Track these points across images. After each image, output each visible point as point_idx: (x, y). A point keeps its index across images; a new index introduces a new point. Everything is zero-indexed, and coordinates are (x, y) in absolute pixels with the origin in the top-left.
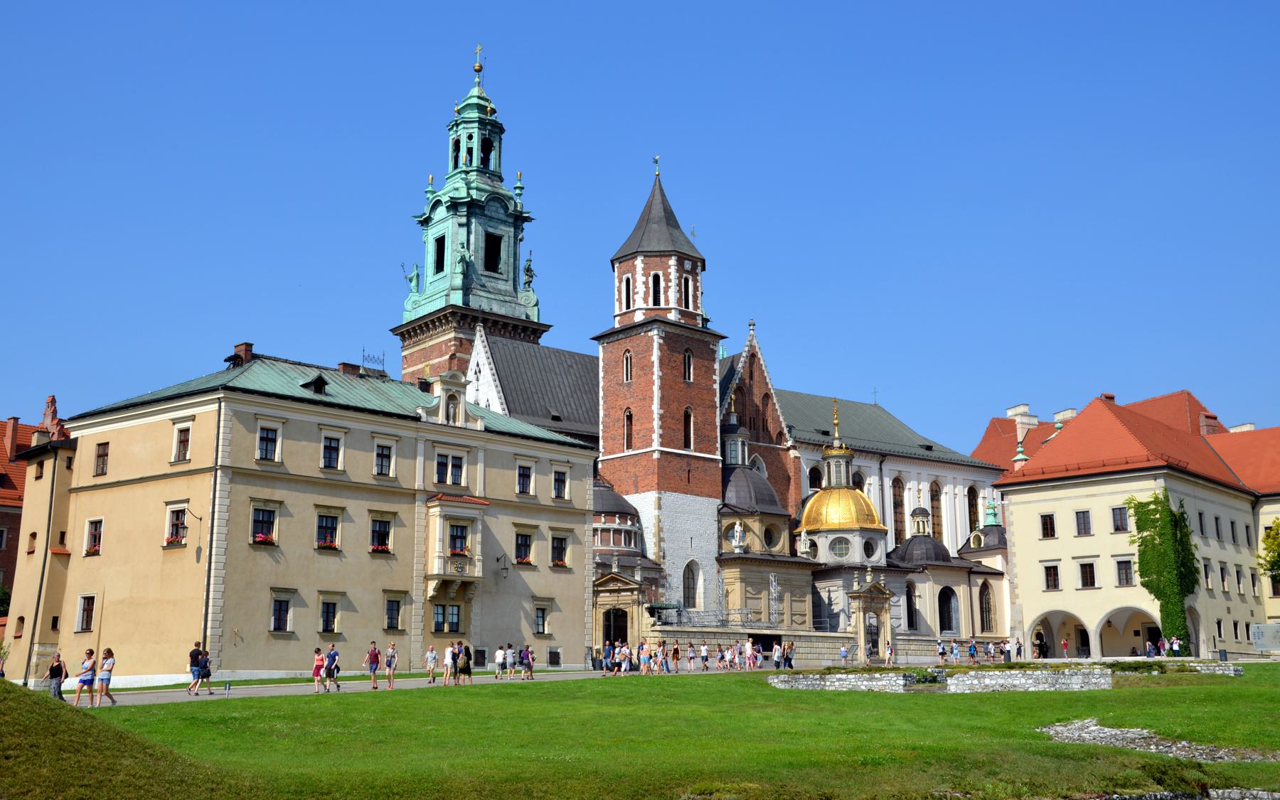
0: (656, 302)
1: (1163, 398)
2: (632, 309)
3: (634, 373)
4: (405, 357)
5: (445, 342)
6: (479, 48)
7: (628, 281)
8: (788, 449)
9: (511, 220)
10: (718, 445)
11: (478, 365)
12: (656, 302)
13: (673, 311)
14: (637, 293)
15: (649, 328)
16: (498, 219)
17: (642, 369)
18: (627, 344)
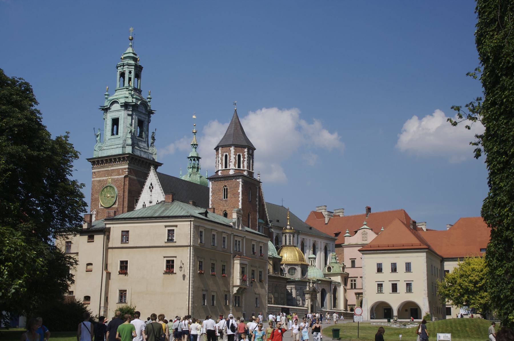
0: (239, 167)
1: (393, 211)
2: (228, 168)
3: (229, 196)
4: (94, 172)
5: (122, 169)
6: (131, 29)
7: (226, 156)
8: (269, 228)
9: (147, 113)
10: (257, 228)
11: (151, 184)
12: (239, 167)
13: (246, 171)
14: (231, 162)
15: (238, 178)
16: (143, 113)
17: (233, 194)
18: (226, 183)
